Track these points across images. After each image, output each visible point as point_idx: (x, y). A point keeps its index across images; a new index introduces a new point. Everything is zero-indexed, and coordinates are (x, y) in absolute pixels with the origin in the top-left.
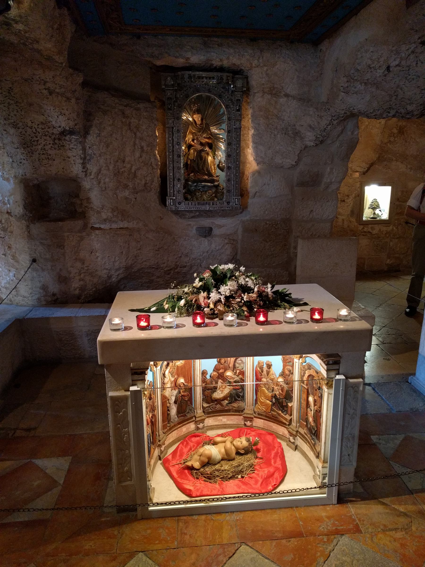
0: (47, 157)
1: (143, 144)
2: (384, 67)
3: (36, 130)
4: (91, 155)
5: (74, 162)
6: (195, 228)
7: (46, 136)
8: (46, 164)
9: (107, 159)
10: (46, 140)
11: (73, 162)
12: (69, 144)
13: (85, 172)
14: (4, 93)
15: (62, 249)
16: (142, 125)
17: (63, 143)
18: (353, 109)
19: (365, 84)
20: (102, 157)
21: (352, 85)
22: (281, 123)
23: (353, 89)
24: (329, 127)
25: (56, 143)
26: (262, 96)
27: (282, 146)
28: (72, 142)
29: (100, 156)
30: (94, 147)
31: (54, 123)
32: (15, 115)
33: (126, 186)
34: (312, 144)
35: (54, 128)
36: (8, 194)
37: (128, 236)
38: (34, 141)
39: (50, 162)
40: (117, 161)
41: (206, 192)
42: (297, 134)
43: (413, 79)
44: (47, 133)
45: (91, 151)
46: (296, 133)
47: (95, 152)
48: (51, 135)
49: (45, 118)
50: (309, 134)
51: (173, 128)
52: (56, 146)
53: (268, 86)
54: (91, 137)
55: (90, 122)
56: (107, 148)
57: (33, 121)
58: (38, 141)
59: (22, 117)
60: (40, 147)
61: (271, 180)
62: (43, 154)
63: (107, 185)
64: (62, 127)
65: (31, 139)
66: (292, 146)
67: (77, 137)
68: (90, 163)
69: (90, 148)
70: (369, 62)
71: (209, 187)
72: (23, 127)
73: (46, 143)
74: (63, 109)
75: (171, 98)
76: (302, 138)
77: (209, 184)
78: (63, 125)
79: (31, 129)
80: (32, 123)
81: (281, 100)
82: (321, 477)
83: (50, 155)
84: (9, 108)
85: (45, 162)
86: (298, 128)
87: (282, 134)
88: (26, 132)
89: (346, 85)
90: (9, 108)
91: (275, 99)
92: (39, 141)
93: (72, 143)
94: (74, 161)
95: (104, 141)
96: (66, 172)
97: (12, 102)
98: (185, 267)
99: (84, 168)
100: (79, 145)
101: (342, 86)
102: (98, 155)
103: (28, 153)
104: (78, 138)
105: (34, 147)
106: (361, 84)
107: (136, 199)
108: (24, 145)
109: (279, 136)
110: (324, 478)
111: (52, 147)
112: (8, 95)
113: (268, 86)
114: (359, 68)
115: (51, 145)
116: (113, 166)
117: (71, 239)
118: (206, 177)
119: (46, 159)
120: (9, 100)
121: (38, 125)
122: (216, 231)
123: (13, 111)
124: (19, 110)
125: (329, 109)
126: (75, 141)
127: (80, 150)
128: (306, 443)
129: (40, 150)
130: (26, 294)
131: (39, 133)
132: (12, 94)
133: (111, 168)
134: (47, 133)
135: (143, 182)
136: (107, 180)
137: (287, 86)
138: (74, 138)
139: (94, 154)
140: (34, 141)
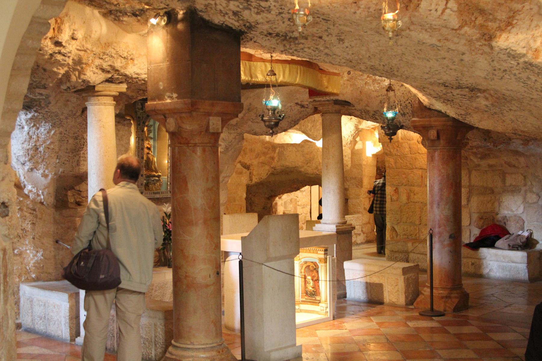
36: (43, 187)
41: (154, 184)
71: (155, 180)
77: (157, 178)
82: (325, 309)
110: (326, 309)
118: (155, 173)
128: (308, 304)
130: (51, 271)
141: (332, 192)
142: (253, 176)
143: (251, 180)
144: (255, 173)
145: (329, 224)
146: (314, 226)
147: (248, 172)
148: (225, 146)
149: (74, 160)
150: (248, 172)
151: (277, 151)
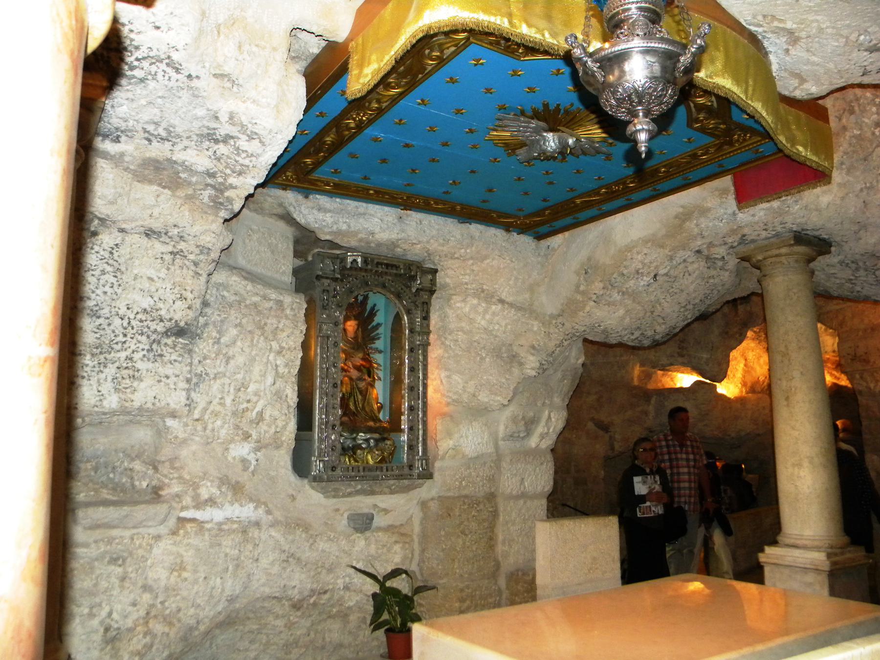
0: (131, 372)
1: (278, 362)
2: (652, 275)
3: (129, 323)
4: (201, 375)
5: (174, 387)
6: (346, 515)
7: (142, 334)
8: (126, 388)
9: (224, 384)
10: (139, 342)
11: (172, 386)
12: (171, 353)
13: (189, 405)
14: (102, 253)
15: (120, 566)
16: (283, 330)
17: (162, 350)
18: (599, 326)
19: (623, 293)
20: (218, 381)
21: (608, 293)
22: (492, 340)
23: (607, 298)
24: (558, 349)
25: (152, 350)
26: (464, 301)
27: (491, 375)
28: (177, 349)
29: (215, 378)
30: (208, 361)
31: (163, 313)
32: (105, 293)
33: (247, 437)
34: (533, 373)
35: (161, 320)
37: (240, 535)
38: (117, 343)
39: (135, 384)
40: (239, 390)
42: (514, 359)
43: (676, 293)
44: (146, 330)
45: (202, 369)
46: (514, 356)
47: (209, 371)
48: (150, 333)
49: (152, 303)
50: (532, 358)
51: (328, 338)
52: (151, 355)
53: (474, 286)
54: (204, 344)
55: (205, 318)
56: (227, 364)
57: (130, 306)
58: (125, 342)
59: (115, 297)
60: (123, 355)
61: (471, 429)
62: (126, 368)
63: (216, 434)
64: (173, 321)
65: (113, 338)
66: (507, 376)
67: (186, 342)
68: (197, 390)
69: (200, 362)
70: (640, 266)
72: (108, 315)
73: (138, 347)
74: (185, 290)
75: (328, 291)
76: (521, 364)
78: (177, 317)
79: (122, 319)
80: (128, 308)
81: (494, 307)
83: (138, 371)
84: (99, 280)
85: (126, 384)
86: (515, 348)
87: (493, 356)
88: (109, 325)
89: (601, 293)
90: (99, 280)
91: (483, 305)
92: (127, 343)
93: (176, 351)
94: (175, 384)
95: (224, 352)
96: (158, 404)
97: (109, 269)
98: (325, 592)
99: (188, 399)
100: (186, 356)
101: (595, 294)
102: (212, 376)
103: (96, 366)
104: (187, 344)
105: (113, 354)
106: (618, 293)
107: (257, 461)
108: (95, 350)
109: (487, 360)
111: (144, 356)
112: (107, 255)
113: (474, 286)
114: (625, 272)
115: (145, 352)
116: (232, 397)
117: (138, 543)
119: (130, 377)
120: (106, 265)
121: (137, 313)
122: (379, 521)
123: (104, 286)
124: (116, 284)
125: (563, 325)
126: (181, 348)
127: (186, 366)
129: (122, 359)
131: (133, 328)
132: (116, 254)
133: (228, 401)
134: (146, 330)
135: (273, 430)
136: (219, 423)
137: (502, 289)
138: (182, 344)
139: (207, 374)
140: (117, 343)
141: (806, 464)
142: (615, 443)
143: (612, 449)
144: (618, 436)
145: (805, 547)
146: (762, 551)
147: (607, 437)
148: (538, 364)
149: (102, 376)
150: (607, 437)
151: (653, 401)
